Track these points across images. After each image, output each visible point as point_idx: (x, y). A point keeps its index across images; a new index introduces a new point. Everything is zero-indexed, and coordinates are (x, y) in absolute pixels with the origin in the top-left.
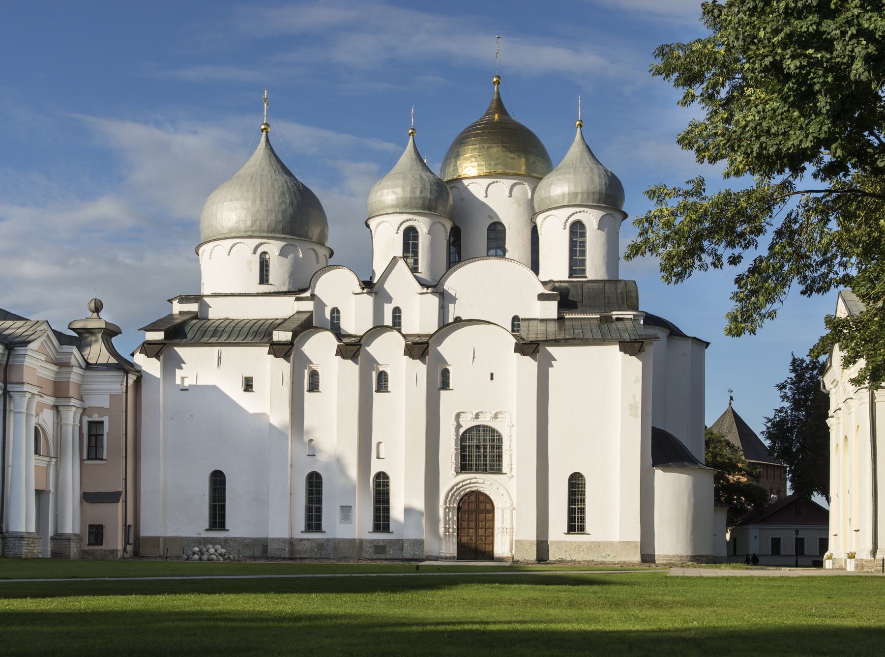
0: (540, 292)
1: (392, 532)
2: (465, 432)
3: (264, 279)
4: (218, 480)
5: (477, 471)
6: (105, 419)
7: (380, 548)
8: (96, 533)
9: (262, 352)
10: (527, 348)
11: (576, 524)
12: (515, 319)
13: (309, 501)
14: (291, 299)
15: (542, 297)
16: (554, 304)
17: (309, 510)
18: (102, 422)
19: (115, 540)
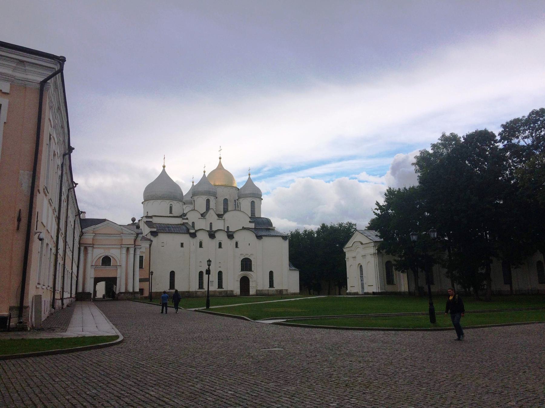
0: (249, 221)
1: (223, 288)
2: (242, 260)
3: (171, 212)
4: (172, 274)
5: (246, 271)
6: (144, 255)
7: (220, 293)
8: (141, 290)
9: (188, 236)
10: (259, 237)
11: (271, 285)
12: (243, 227)
13: (199, 280)
14: (181, 219)
15: (250, 222)
16: (253, 224)
17: (199, 282)
18: (143, 256)
19: (146, 294)
